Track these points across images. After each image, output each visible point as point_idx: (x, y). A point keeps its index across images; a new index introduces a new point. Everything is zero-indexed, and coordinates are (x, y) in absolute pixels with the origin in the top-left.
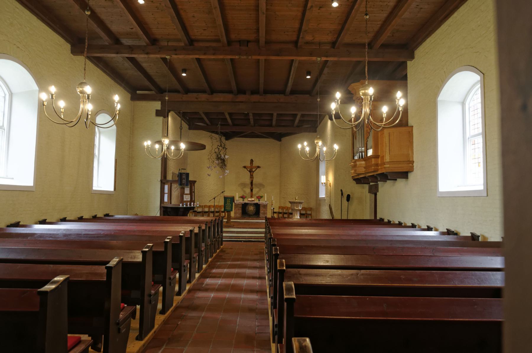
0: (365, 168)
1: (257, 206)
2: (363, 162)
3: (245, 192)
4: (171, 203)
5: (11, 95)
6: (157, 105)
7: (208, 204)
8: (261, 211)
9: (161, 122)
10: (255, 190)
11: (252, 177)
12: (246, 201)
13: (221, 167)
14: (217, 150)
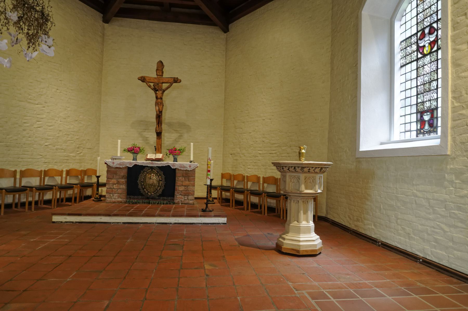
1: (169, 174)
8: (180, 188)
11: (159, 101)
12: (141, 161)
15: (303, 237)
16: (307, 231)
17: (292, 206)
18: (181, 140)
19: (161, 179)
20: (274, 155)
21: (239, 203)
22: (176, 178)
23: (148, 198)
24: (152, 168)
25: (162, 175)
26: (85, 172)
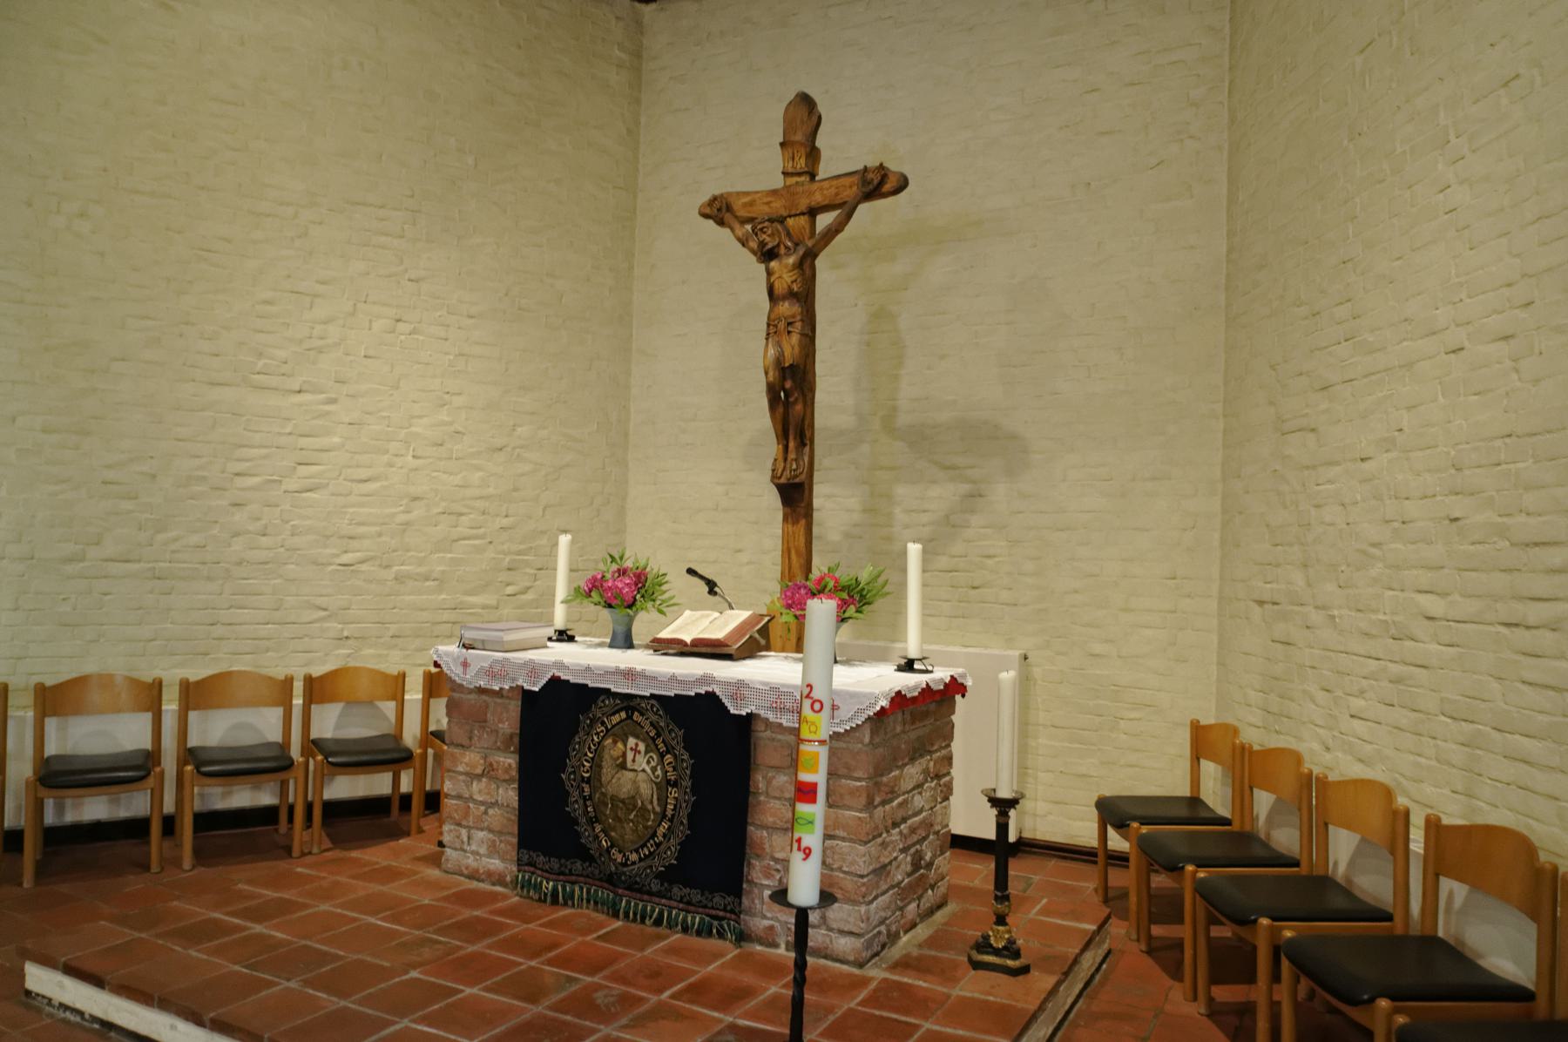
1: (715, 743)
18: (975, 520)
19: (672, 776)
20: (1546, 639)
22: (759, 780)
23: (611, 880)
24: (628, 702)
25: (680, 750)
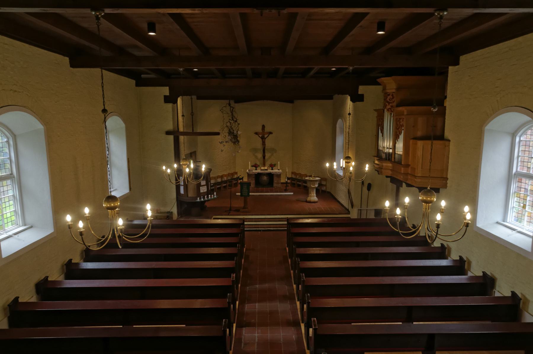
0: (391, 170)
2: (391, 165)
3: (256, 157)
4: (187, 196)
5: (15, 137)
6: (166, 91)
7: (220, 175)
9: (171, 110)
10: (267, 155)
11: (264, 143)
12: (259, 171)
13: (234, 143)
14: (228, 124)
15: (312, 198)
16: (314, 196)
17: (310, 190)
21: (299, 186)
26: (233, 174)
